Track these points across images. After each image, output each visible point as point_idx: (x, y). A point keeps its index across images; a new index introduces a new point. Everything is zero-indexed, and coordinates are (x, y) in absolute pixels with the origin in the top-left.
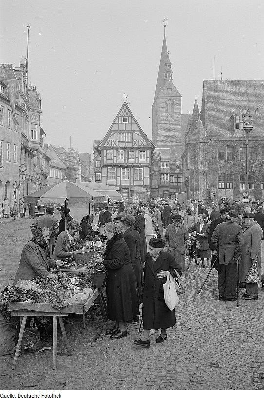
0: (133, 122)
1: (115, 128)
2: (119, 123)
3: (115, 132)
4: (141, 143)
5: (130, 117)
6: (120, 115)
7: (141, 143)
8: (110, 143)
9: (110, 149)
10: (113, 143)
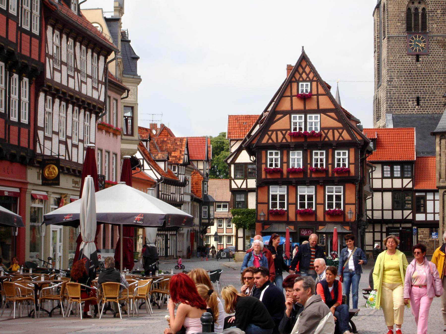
0: (321, 91)
1: (285, 105)
2: (291, 96)
3: (285, 113)
4: (337, 134)
5: (314, 84)
6: (294, 79)
7: (337, 134)
8: (274, 137)
9: (273, 147)
10: (280, 136)
